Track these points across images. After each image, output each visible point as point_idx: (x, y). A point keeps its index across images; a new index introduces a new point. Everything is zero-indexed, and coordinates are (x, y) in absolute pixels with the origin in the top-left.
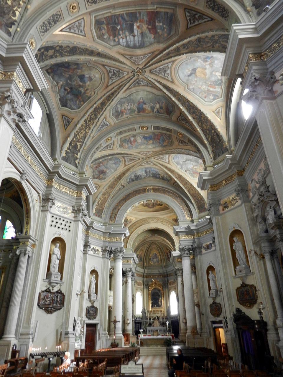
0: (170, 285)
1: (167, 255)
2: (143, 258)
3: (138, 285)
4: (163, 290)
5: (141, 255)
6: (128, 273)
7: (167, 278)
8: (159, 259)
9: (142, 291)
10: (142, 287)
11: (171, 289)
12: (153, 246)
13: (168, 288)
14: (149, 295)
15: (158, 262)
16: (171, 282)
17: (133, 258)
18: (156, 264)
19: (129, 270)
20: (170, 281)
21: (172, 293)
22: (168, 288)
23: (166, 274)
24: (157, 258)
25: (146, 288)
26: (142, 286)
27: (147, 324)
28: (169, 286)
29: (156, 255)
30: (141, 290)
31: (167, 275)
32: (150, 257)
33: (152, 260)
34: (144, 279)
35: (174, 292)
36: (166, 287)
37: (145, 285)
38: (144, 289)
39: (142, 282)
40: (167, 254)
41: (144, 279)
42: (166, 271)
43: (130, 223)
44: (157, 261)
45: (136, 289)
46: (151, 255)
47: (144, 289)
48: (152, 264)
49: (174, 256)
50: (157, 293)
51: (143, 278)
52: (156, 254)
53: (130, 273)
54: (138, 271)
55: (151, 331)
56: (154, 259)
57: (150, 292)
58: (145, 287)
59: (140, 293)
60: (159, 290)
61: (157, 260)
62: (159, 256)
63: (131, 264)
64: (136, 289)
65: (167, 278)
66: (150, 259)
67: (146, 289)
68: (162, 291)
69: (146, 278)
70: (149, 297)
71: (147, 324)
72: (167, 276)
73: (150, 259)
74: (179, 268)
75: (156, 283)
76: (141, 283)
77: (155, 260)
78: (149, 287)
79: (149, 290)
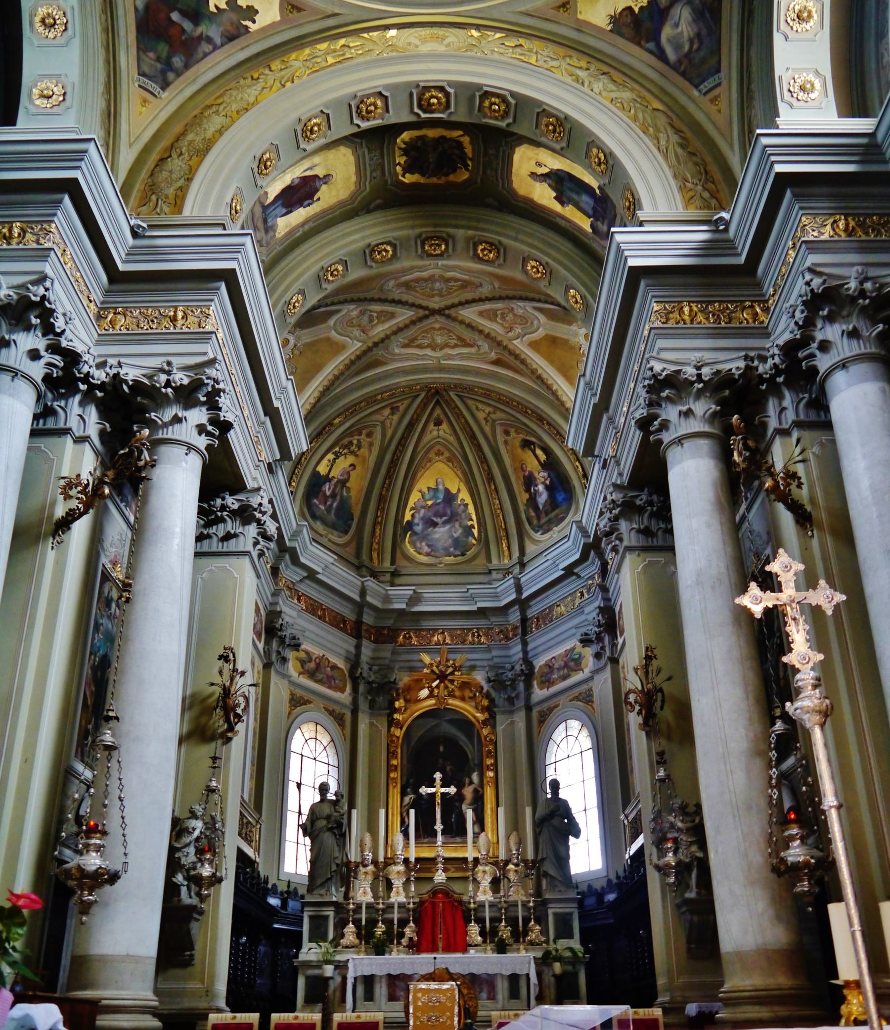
0: (547, 682)
1: (523, 497)
2: (357, 513)
3: (312, 675)
4: (491, 721)
5: (343, 483)
6: (168, 414)
7: (525, 644)
8: (468, 530)
9: (339, 719)
10: (345, 697)
11: (551, 710)
12: (433, 432)
13: (529, 708)
14: (391, 754)
15: (460, 546)
16: (549, 666)
17: (229, 278)
18: (450, 560)
19: (181, 378)
20: (539, 663)
21: (559, 733)
22: (529, 708)
23: (514, 616)
24: (453, 518)
25: (372, 705)
26: (342, 691)
27: (350, 928)
28: (539, 693)
29: (450, 498)
30: (331, 713)
31: (524, 620)
32: (408, 517)
33: (424, 537)
34: (358, 647)
35: (574, 724)
36: (511, 701)
37: (362, 688)
38: (355, 712)
39: (341, 664)
40: (529, 482)
41: (358, 647)
42: (519, 589)
43: (230, 38)
44: (456, 542)
45: (297, 702)
46: (414, 498)
47: (355, 712)
48: (423, 559)
49: (637, 274)
50: (451, 742)
51: (353, 641)
52: (447, 491)
53: (198, 416)
54: (312, 575)
55: (381, 991)
56: (435, 525)
57: (398, 733)
58: (363, 705)
59: (325, 739)
60: (465, 724)
61: (458, 532)
62: (471, 509)
63: (205, 336)
64: (297, 702)
65: (525, 644)
66: (410, 525)
67: (372, 715)
68: (485, 732)
69: (376, 641)
70: (390, 768)
71: (350, 928)
72: (525, 633)
73: (410, 525)
74: (690, 372)
75: (442, 677)
76: (334, 667)
77: (442, 534)
78: (391, 703)
79: (391, 723)
